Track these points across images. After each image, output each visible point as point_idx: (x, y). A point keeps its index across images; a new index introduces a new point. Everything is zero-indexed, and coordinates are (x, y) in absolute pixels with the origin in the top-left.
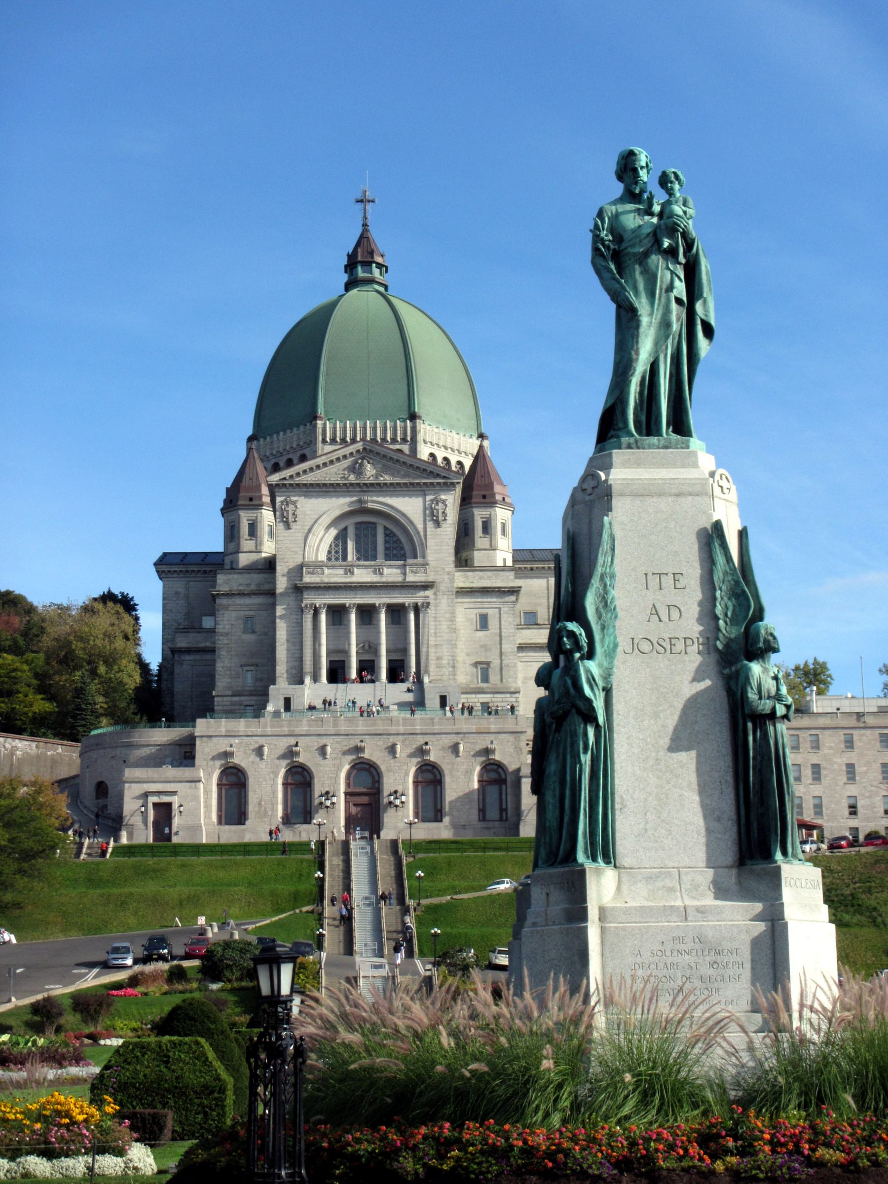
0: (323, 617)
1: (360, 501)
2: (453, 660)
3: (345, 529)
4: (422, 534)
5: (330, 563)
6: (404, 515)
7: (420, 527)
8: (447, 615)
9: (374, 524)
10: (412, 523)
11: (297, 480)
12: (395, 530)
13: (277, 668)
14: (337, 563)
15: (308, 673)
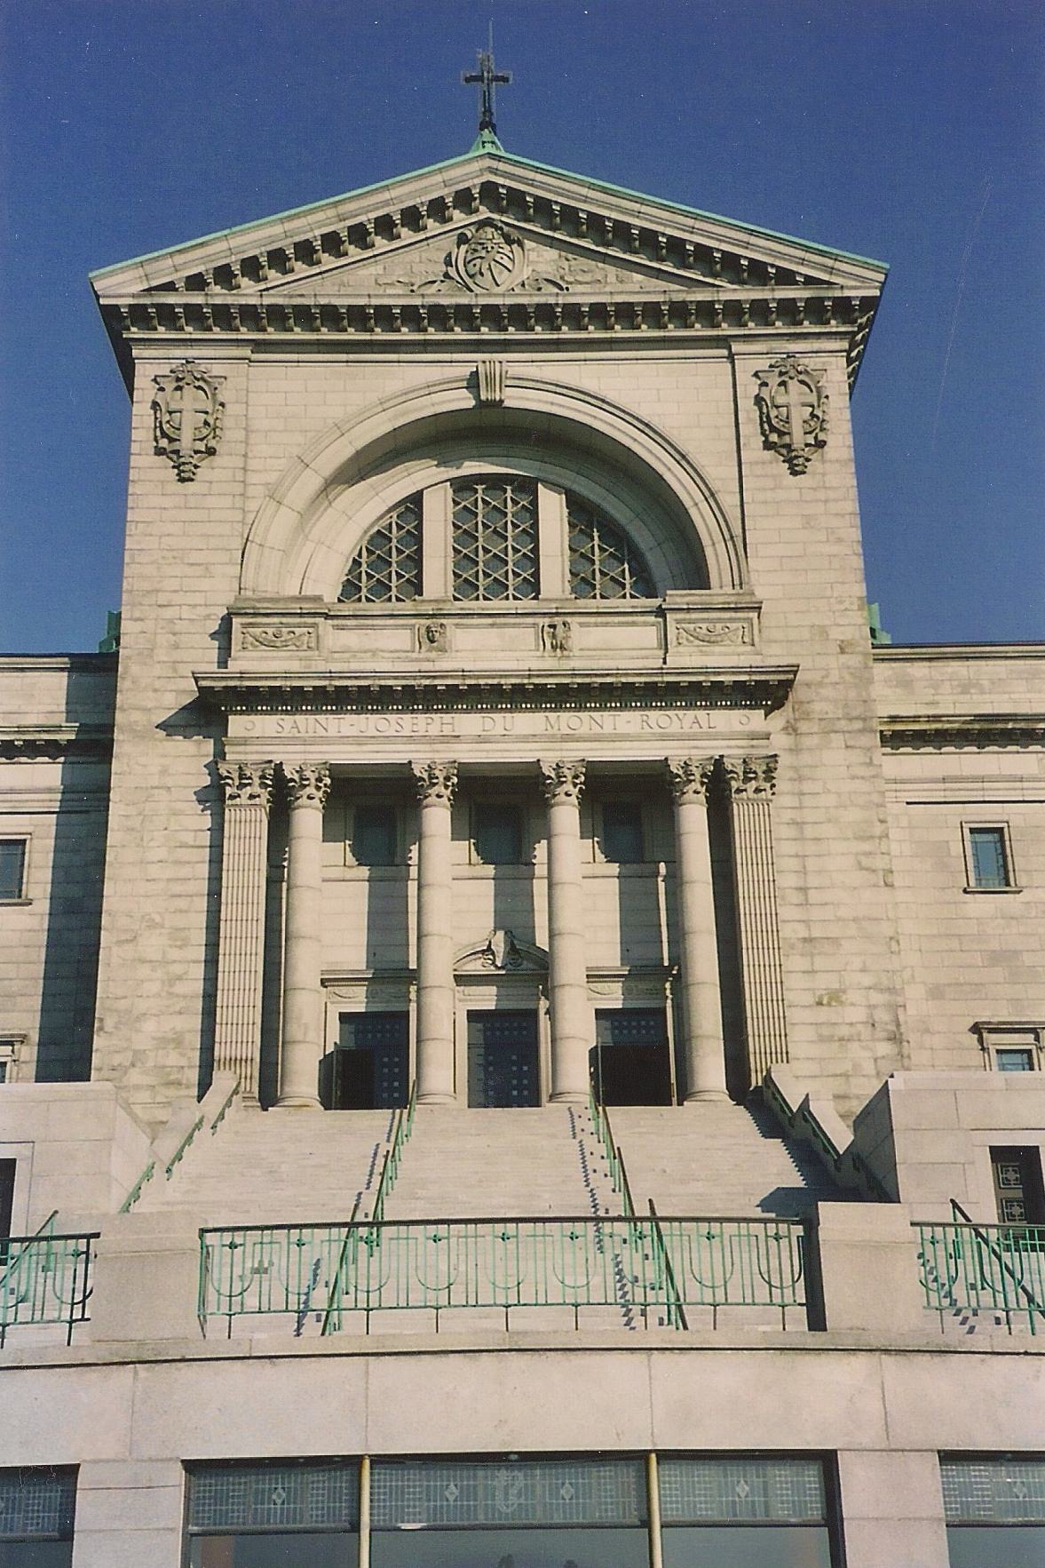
0: (308, 818)
1: (473, 383)
2: (895, 1008)
3: (416, 500)
4: (730, 501)
5: (348, 608)
6: (647, 428)
7: (721, 474)
8: (853, 815)
9: (527, 487)
10: (682, 458)
11: (218, 295)
12: (618, 510)
13: (98, 1042)
14: (378, 607)
15: (234, 1061)
